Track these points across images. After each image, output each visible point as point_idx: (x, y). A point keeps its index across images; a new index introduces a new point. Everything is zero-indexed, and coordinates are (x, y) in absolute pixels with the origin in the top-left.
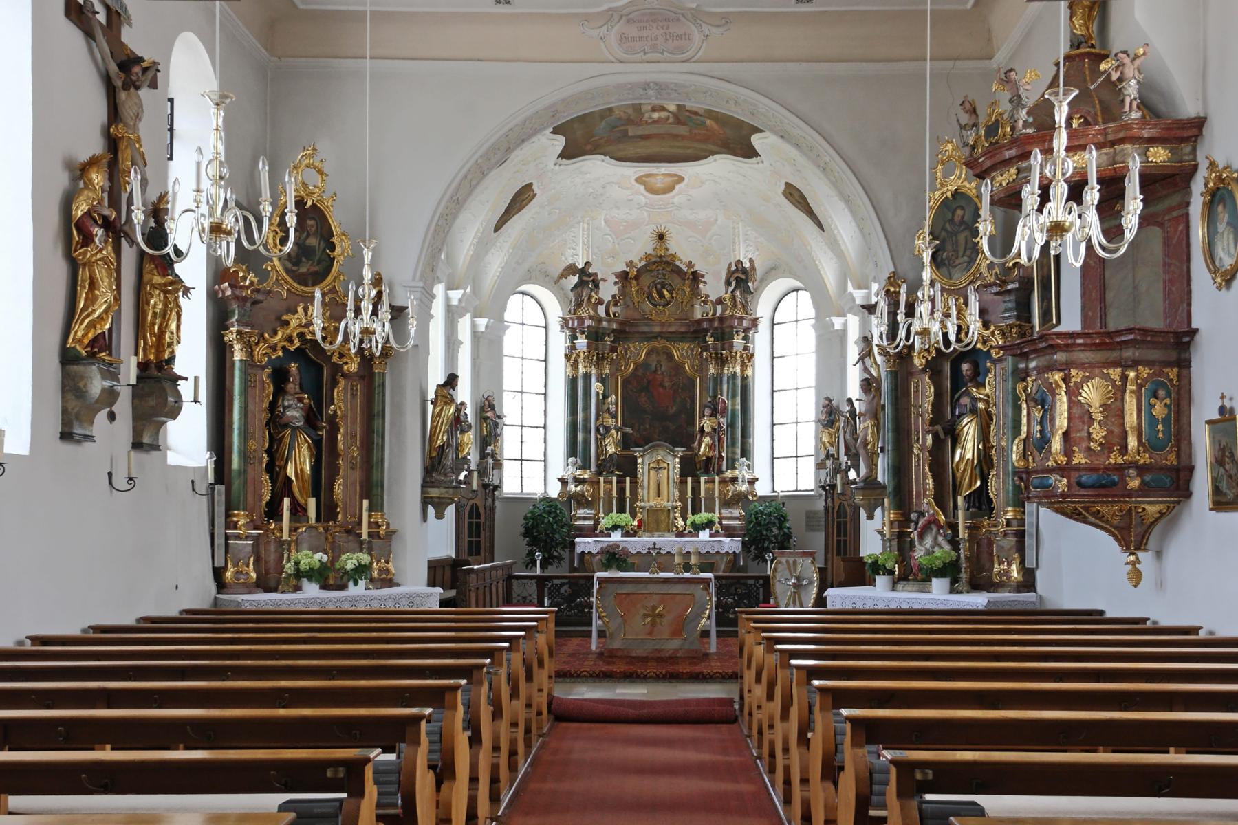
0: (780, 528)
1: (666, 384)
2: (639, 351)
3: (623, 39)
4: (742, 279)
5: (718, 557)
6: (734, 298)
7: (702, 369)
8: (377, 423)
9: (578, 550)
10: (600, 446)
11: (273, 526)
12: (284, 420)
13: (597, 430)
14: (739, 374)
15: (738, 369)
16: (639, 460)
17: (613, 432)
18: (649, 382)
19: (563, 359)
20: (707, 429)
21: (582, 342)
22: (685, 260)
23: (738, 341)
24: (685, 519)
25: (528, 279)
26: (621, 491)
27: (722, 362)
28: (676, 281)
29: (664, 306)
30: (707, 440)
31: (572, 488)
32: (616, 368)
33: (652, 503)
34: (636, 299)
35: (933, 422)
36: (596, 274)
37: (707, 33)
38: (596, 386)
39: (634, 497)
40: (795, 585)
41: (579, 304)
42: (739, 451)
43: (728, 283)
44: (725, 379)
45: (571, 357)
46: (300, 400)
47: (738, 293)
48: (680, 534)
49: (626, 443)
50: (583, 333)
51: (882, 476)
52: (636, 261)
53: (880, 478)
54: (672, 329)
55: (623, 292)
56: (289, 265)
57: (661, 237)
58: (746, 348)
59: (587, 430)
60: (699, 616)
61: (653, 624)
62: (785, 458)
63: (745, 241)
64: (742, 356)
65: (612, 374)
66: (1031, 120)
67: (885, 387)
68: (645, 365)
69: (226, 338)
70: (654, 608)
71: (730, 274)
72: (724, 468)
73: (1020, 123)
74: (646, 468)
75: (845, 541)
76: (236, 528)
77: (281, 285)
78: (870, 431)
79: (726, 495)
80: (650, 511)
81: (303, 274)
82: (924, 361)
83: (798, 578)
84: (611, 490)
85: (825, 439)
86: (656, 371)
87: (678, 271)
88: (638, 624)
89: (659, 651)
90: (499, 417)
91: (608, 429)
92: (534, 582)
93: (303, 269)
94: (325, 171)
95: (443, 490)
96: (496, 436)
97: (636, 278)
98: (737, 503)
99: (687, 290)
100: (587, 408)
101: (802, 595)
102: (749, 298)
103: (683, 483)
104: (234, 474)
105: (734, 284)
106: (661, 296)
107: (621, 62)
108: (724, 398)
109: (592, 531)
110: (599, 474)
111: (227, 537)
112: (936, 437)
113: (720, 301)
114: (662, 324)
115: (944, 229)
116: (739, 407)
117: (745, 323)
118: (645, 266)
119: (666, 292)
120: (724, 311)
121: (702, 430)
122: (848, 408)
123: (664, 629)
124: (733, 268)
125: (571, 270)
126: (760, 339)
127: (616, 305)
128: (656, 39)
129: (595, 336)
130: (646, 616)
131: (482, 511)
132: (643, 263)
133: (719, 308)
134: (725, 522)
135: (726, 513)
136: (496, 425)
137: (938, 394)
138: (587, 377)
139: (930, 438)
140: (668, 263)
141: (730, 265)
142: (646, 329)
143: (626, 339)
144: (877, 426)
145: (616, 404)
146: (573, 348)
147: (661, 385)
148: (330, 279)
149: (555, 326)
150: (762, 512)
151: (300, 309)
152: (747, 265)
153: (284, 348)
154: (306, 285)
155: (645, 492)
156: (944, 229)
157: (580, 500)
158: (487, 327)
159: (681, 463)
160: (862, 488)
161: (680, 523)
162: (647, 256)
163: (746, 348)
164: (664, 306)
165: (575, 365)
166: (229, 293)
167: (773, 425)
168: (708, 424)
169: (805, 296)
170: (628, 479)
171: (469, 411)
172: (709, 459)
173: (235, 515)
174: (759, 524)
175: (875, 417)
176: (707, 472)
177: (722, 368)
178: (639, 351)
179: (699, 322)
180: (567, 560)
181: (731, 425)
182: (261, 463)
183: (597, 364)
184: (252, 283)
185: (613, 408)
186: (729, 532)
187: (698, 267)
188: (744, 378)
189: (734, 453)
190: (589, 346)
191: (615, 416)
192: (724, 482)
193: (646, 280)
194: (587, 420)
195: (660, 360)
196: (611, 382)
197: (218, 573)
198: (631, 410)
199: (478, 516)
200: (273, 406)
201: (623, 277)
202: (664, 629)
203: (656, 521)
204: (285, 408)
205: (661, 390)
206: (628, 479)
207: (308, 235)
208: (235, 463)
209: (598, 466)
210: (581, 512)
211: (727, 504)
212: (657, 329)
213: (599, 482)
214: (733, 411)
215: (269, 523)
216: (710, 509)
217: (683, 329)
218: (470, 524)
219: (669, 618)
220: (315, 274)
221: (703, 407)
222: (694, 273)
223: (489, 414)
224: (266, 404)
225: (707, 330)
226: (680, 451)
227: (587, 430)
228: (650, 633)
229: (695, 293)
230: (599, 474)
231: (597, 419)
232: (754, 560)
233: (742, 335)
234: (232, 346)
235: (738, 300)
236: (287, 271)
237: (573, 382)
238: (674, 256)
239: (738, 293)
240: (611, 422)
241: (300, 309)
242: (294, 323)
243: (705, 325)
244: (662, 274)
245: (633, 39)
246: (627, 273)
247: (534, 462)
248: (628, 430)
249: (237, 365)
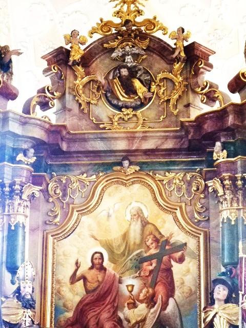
22: (173, 28)
28: (158, 66)
34: (83, 98)
52: (84, 32)
54: (149, 145)
87: (162, 50)
106: (130, 90)
114: (131, 137)
118: (102, 42)
119: (137, 84)
127: (45, 105)
132: (97, 36)
140: (142, 36)
142: (99, 146)
143: (67, 168)
162: (106, 25)
164: (135, 108)
185: (27, 291)
201: (60, 58)
212: (121, 145)
217: (169, 145)
222: (191, 50)
225: (212, 138)
238: (151, 23)
243: (208, 127)
246: (68, 53)
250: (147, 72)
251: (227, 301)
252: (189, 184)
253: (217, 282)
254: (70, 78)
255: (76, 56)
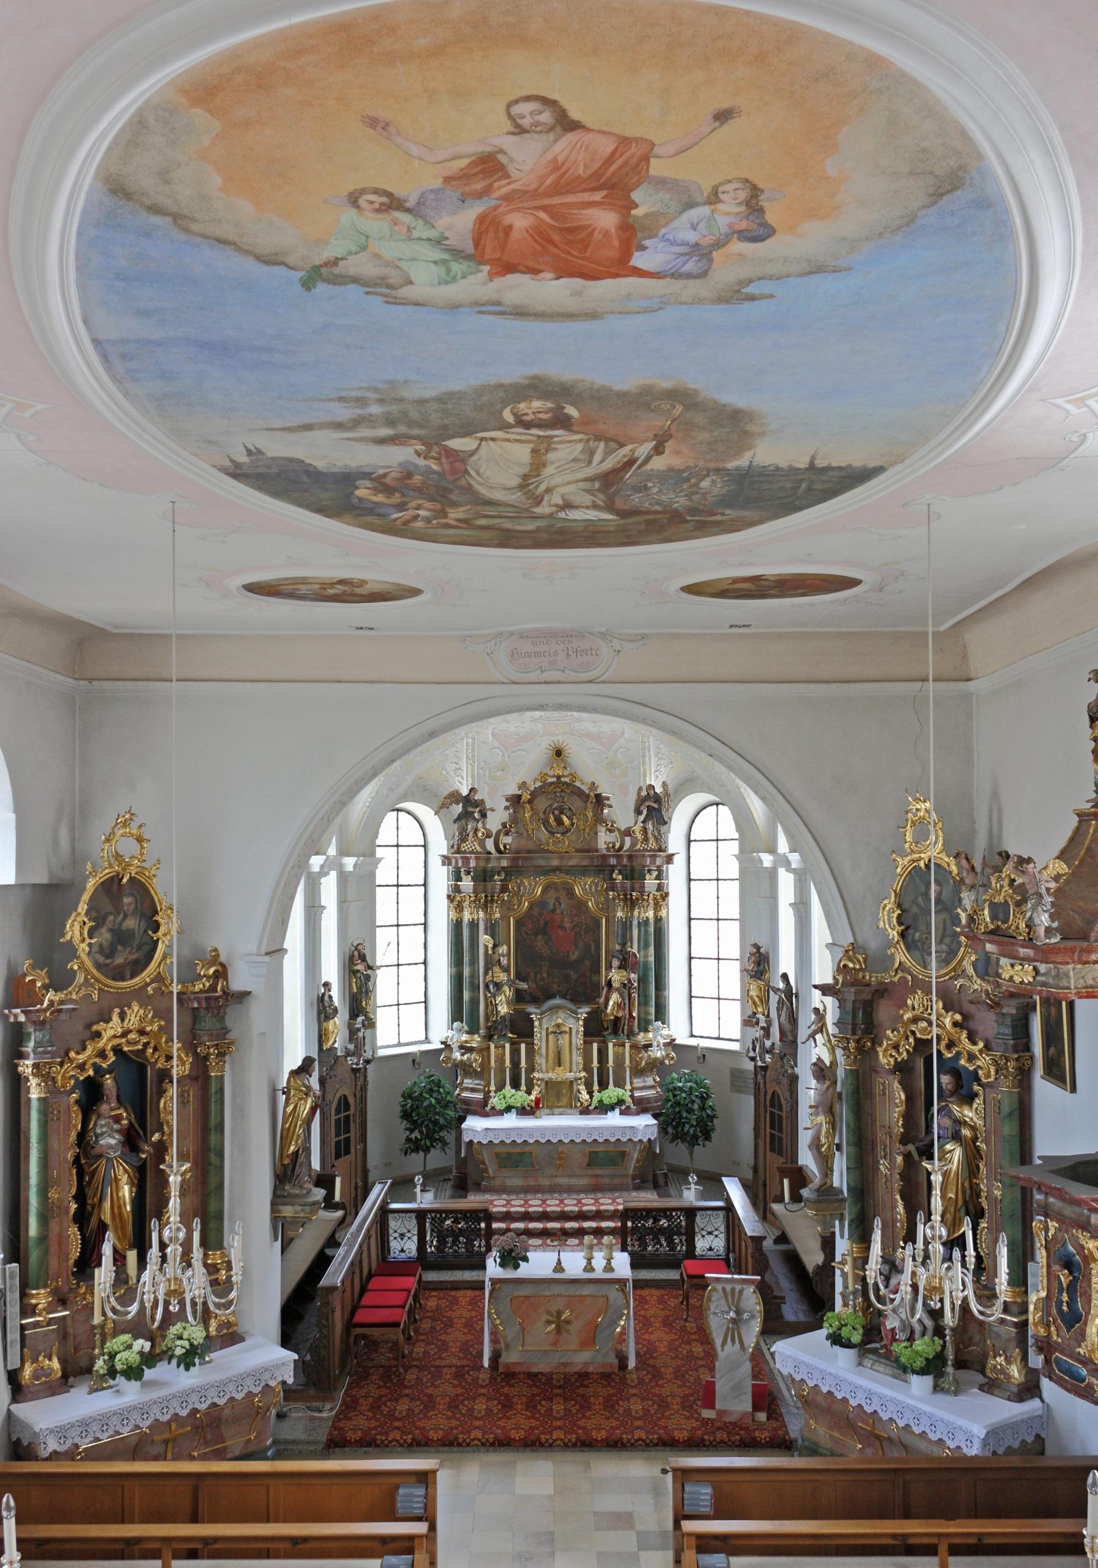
0: (703, 1109)
1: (567, 925)
2: (534, 888)
3: (514, 654)
4: (654, 808)
5: (630, 1144)
6: (645, 830)
7: (608, 908)
8: (213, 1139)
9: (466, 1138)
10: (491, 1007)
11: (83, 1290)
12: (97, 1151)
13: (487, 986)
14: (652, 921)
15: (651, 914)
16: (536, 1023)
17: (506, 988)
18: (546, 923)
19: (445, 901)
20: (616, 985)
21: (467, 884)
23: (650, 882)
24: (591, 1093)
25: (405, 798)
26: (516, 1063)
27: (631, 904)
28: (577, 804)
29: (563, 834)
30: (615, 997)
31: (457, 1055)
32: (508, 907)
33: (551, 1075)
34: (530, 827)
35: (904, 1140)
36: (482, 802)
37: (618, 647)
38: (485, 939)
39: (531, 1069)
40: (734, 1321)
41: (463, 839)
42: (652, 1010)
43: (638, 812)
44: (635, 923)
45: (454, 897)
46: (117, 1119)
47: (650, 826)
48: (585, 1111)
49: (520, 997)
50: (468, 873)
51: (840, 1179)
52: (529, 782)
53: (836, 1184)
54: (573, 862)
55: (514, 820)
56: (101, 959)
57: (559, 753)
58: (660, 888)
59: (474, 988)
60: (615, 1323)
61: (558, 1330)
62: (705, 1010)
63: (657, 754)
64: (655, 899)
65: (502, 918)
66: (1055, 925)
67: (840, 1073)
68: (540, 903)
69: (20, 1069)
70: (559, 1313)
71: (641, 801)
72: (636, 1030)
73: (1041, 931)
74: (544, 1033)
75: (780, 1139)
76: (33, 1314)
77: (92, 985)
78: (824, 1130)
79: (638, 1064)
80: (548, 1084)
81: (119, 966)
82: (892, 1061)
83: (738, 1312)
84: (504, 1055)
85: (753, 993)
86: (554, 910)
87: (579, 793)
88: (542, 1331)
89: (566, 1365)
90: (370, 968)
91: (498, 986)
92: (413, 1215)
93: (119, 960)
94: (145, 836)
95: (298, 1208)
96: (368, 992)
97: (530, 802)
98: (652, 1069)
99: (590, 814)
100: (474, 961)
101: (743, 1332)
102: (663, 829)
103: (587, 1043)
104: (31, 1243)
105: (645, 812)
106: (560, 822)
107: (514, 683)
108: (635, 950)
109: (482, 1109)
110: (489, 1037)
111: (23, 1328)
112: (907, 1157)
113: (628, 832)
115: (914, 902)
116: (652, 959)
117: (658, 861)
119: (565, 818)
120: (633, 844)
121: (609, 984)
122: (781, 985)
123: (572, 1339)
124: (644, 793)
125: (454, 797)
126: (675, 874)
127: (507, 834)
128: (556, 654)
129: (482, 877)
130: (549, 1322)
131: (351, 1100)
132: (538, 784)
133: (628, 840)
134: (637, 1094)
135: (638, 1082)
136: (368, 978)
137: (910, 1099)
138: (473, 925)
139: (899, 1159)
141: (640, 789)
142: (542, 863)
144: (833, 1125)
145: (509, 954)
146: (457, 889)
147: (561, 927)
148: (153, 965)
149: (435, 862)
150: (681, 1089)
151: (115, 1018)
152: (659, 790)
153: (94, 1065)
154: (123, 979)
155: (543, 1061)
156: (914, 902)
157: (466, 1069)
158: (355, 866)
159: (585, 1026)
160: (816, 1202)
161: (585, 1096)
163: (660, 888)
165: (459, 908)
166: (22, 1018)
167: (690, 958)
168: (617, 977)
169: (724, 810)
170: (523, 1046)
171: (335, 993)
172: (617, 1019)
173: (33, 1296)
174: (678, 1104)
175: (830, 1111)
176: (615, 1033)
177: (632, 910)
178: (534, 888)
179: (604, 857)
180: (452, 1145)
181: (643, 980)
182: (67, 1213)
183: (485, 907)
184: (51, 1003)
186: (642, 1106)
187: (604, 790)
188: (658, 920)
189: (648, 1013)
190: (475, 891)
191: (506, 970)
192: (634, 1047)
193: (542, 803)
194: (474, 976)
195: (559, 916)
196: (501, 931)
197: (13, 1377)
198: (527, 961)
199: (347, 1107)
200: (81, 1137)
201: (515, 801)
202: (572, 1339)
203: (557, 1097)
204: (97, 1136)
205: (560, 932)
206: (523, 1046)
207: (126, 916)
208: (33, 1229)
209: (489, 1028)
210: (468, 1082)
211: (638, 1072)
212: (555, 863)
213: (489, 1048)
214: (646, 964)
215: (78, 1286)
216: (620, 1084)
217: (585, 863)
218: (338, 1121)
219: (576, 1327)
220: (136, 962)
221: (610, 955)
222: (598, 797)
223: (358, 967)
224: (73, 1136)
226: (584, 1011)
227: (474, 988)
228: (555, 1344)
229: (599, 819)
230: (489, 1037)
231: (486, 973)
232: (672, 1141)
233: (655, 873)
234: (28, 1081)
235: (650, 833)
236: (98, 966)
237: (456, 927)
238: (573, 776)
239: (650, 826)
240: (502, 977)
241: (115, 1018)
242: (106, 1036)
243: (613, 861)
244: (560, 798)
245: (528, 655)
246: (520, 797)
247: (413, 1015)
248: (524, 986)
249: (35, 1105)
250: (570, 809)
251: (619, 968)
252: (597, 885)
253: (613, 957)
254: (521, 812)
255: (526, 797)
